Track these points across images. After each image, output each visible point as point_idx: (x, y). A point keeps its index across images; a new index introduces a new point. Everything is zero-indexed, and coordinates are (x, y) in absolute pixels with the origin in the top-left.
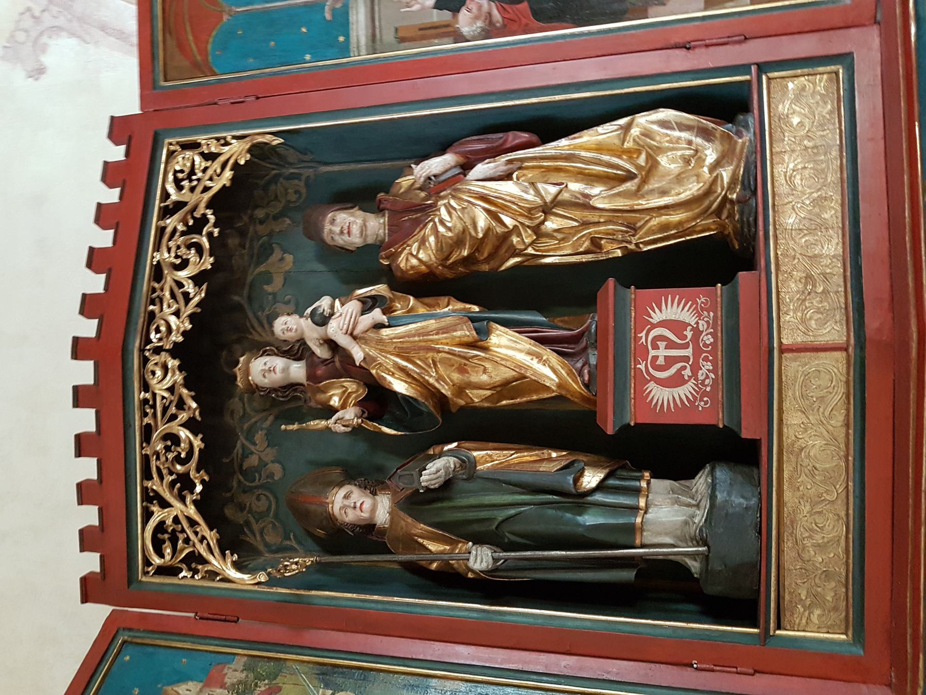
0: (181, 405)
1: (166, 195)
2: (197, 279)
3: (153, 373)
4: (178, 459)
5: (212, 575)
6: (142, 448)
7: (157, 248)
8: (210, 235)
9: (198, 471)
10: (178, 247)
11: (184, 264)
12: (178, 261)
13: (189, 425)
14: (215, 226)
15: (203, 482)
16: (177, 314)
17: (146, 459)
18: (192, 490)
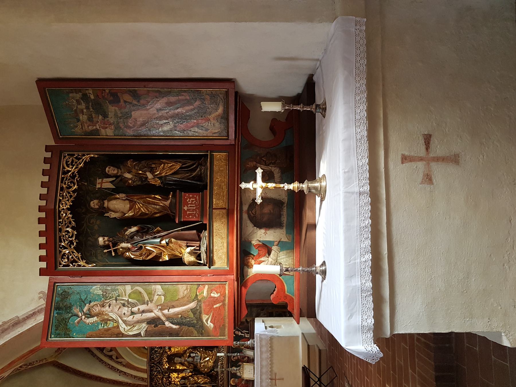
0: (70, 223)
1: (64, 168)
2: (74, 192)
3: (62, 215)
4: (69, 237)
5: (80, 266)
6: (59, 234)
7: (62, 182)
8: (77, 180)
9: (75, 239)
10: (68, 183)
11: (71, 187)
12: (68, 186)
13: (73, 228)
14: (78, 177)
15: (76, 243)
16: (68, 200)
17: (60, 237)
18: (73, 244)
